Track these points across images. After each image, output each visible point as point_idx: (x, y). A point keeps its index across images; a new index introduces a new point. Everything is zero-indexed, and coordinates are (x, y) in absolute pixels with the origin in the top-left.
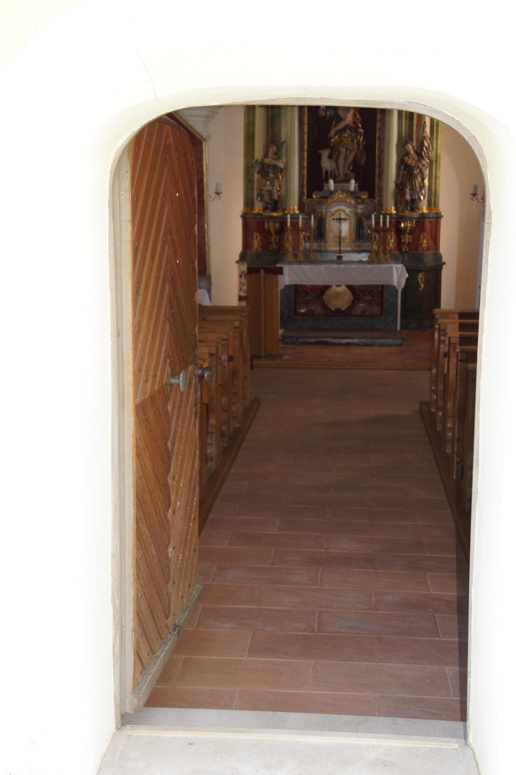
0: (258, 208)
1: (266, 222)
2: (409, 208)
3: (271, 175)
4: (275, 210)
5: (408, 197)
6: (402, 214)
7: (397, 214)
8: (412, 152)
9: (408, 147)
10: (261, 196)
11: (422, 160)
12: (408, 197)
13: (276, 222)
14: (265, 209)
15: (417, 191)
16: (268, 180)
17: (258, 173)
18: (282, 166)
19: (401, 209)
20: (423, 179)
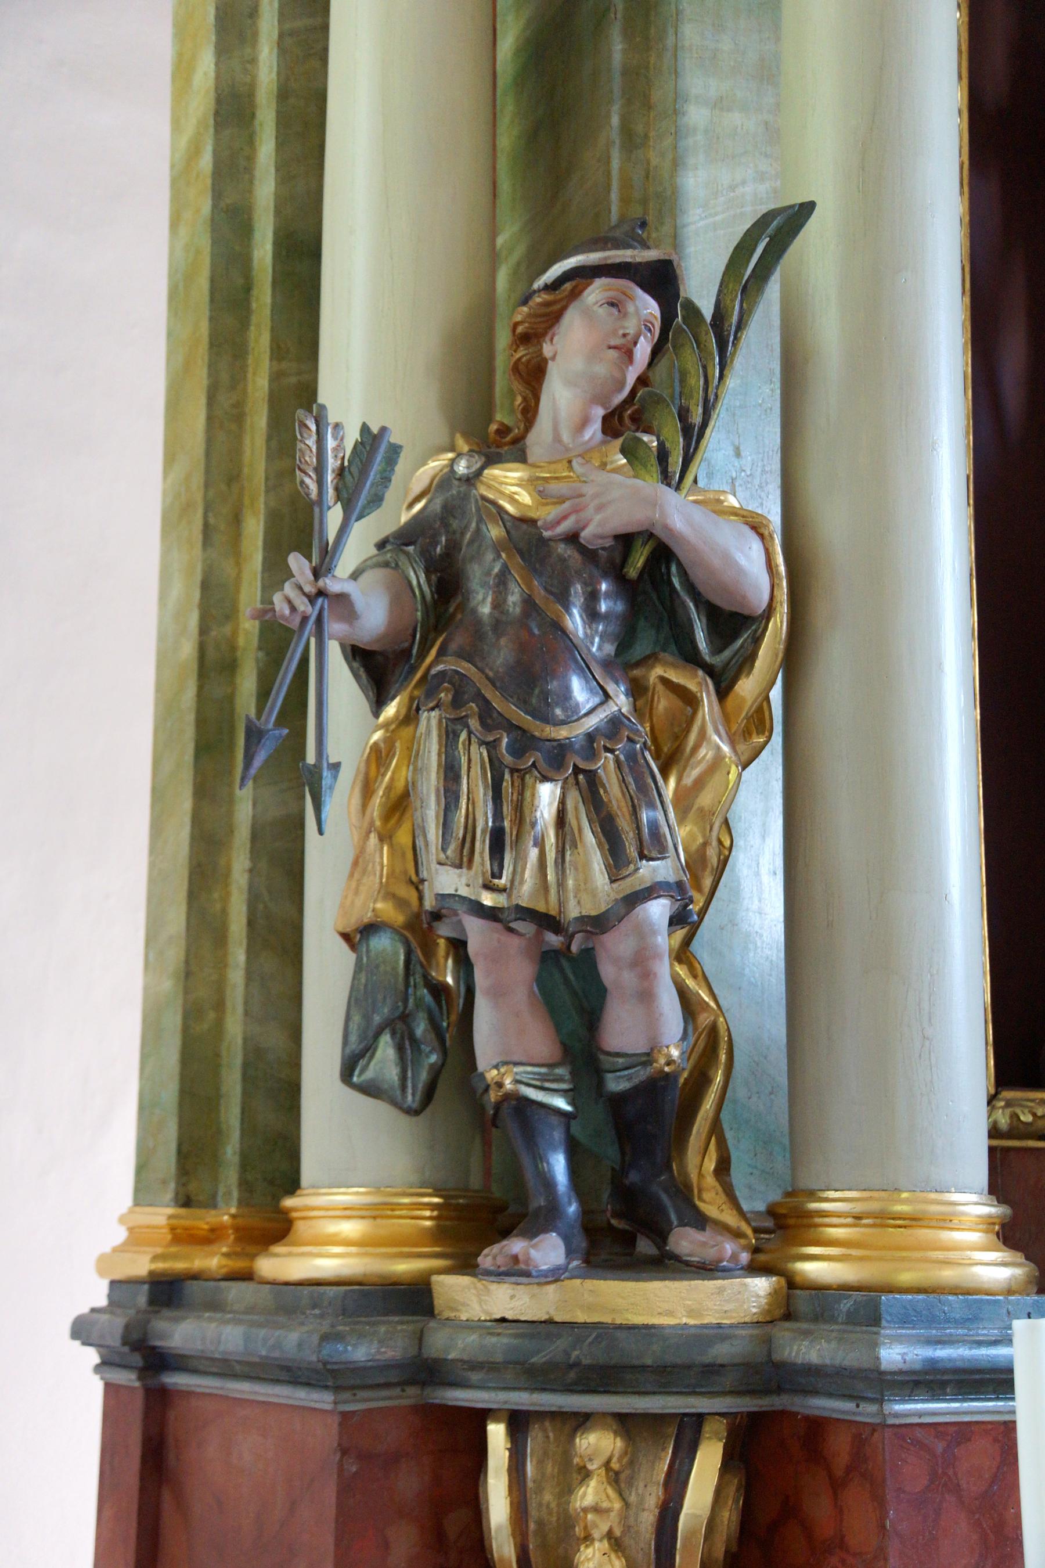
0: (352, 1206)
1: (497, 1433)
3: (587, 701)
4: (629, 1231)
10: (419, 1011)
13: (688, 1433)
14: (479, 1219)
16: (556, 759)
17: (378, 669)
18: (751, 568)
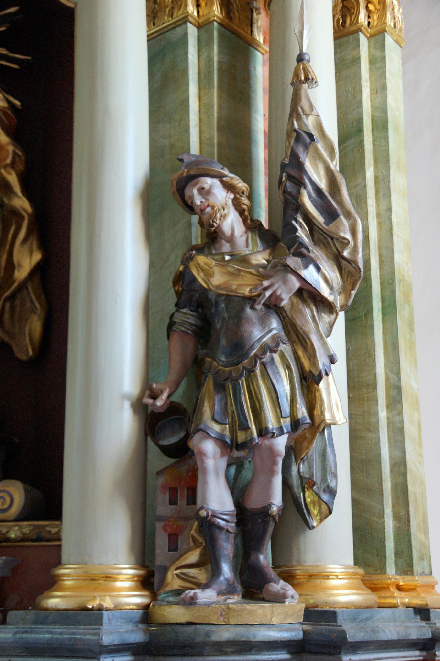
2: (227, 570)
5: (218, 498)
6: (175, 613)
7: (146, 616)
8: (231, 222)
9: (205, 193)
11: (292, 261)
12: (218, 498)
15: (272, 453)
19: (173, 581)
20: (309, 381)
